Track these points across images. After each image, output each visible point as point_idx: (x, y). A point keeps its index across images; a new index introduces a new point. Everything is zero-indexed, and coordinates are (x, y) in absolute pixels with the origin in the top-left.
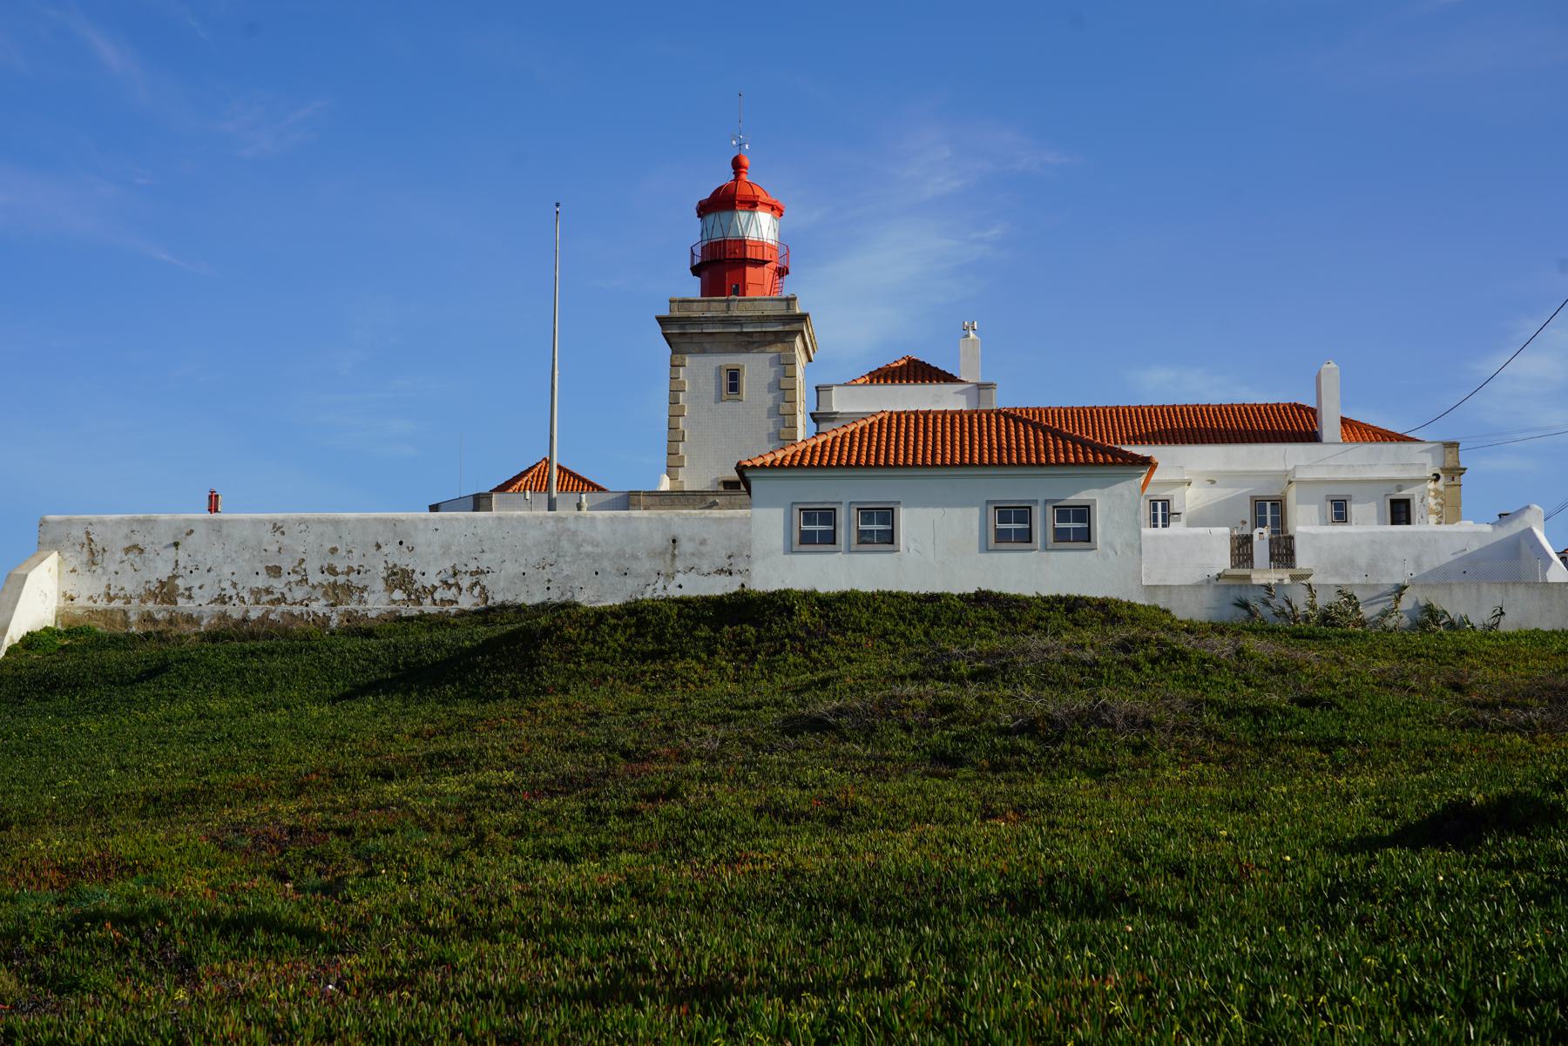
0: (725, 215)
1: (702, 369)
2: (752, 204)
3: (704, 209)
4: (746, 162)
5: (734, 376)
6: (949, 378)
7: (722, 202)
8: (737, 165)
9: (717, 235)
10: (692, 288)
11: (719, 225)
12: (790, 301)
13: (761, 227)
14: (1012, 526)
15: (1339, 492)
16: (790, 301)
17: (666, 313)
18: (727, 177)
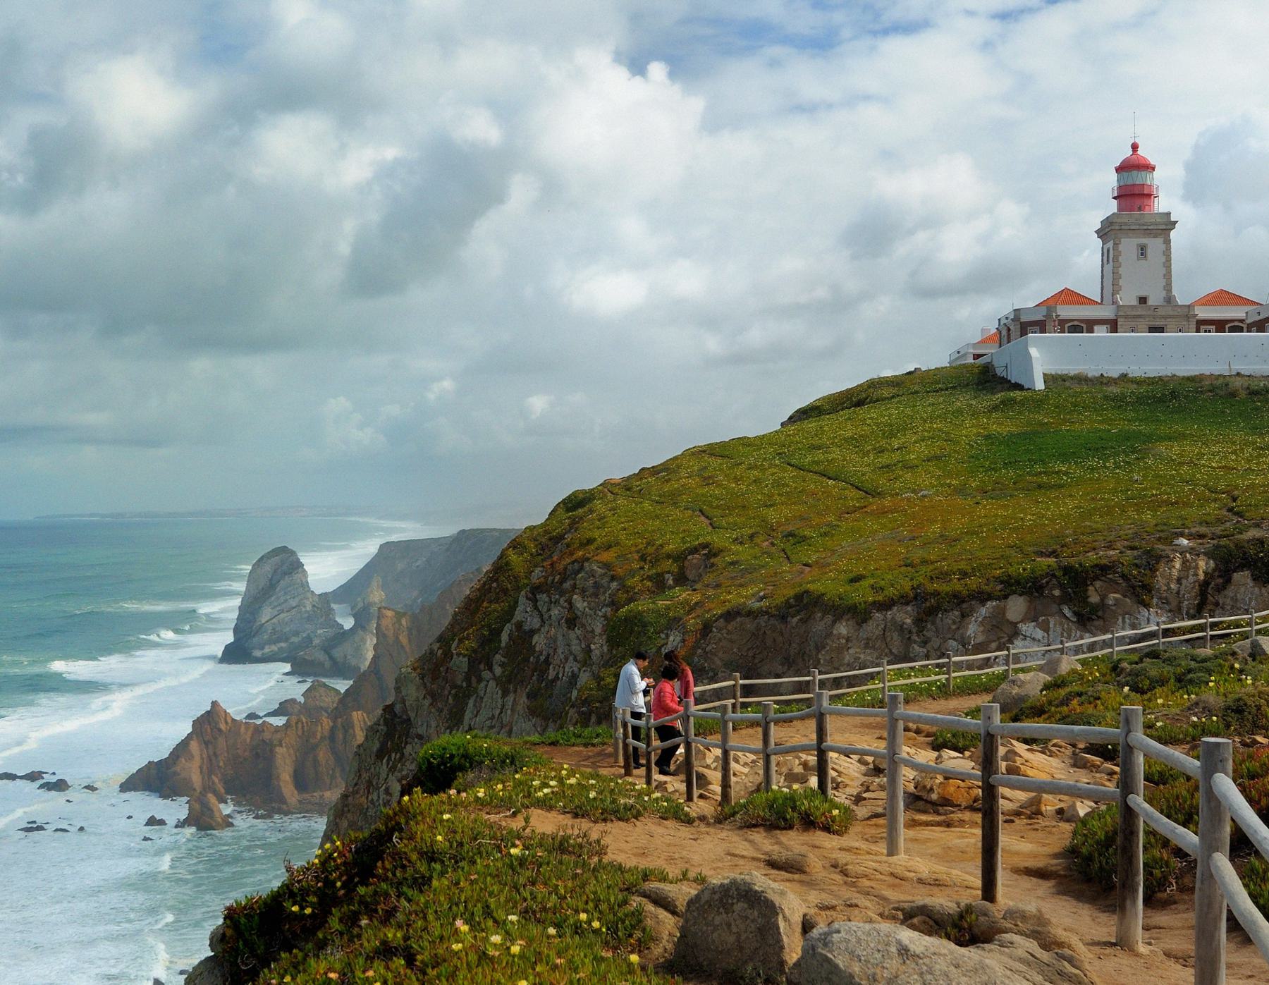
1: (1129, 246)
3: (1118, 170)
5: (1143, 251)
8: (1135, 147)
10: (1113, 207)
12: (1169, 214)
16: (1169, 214)
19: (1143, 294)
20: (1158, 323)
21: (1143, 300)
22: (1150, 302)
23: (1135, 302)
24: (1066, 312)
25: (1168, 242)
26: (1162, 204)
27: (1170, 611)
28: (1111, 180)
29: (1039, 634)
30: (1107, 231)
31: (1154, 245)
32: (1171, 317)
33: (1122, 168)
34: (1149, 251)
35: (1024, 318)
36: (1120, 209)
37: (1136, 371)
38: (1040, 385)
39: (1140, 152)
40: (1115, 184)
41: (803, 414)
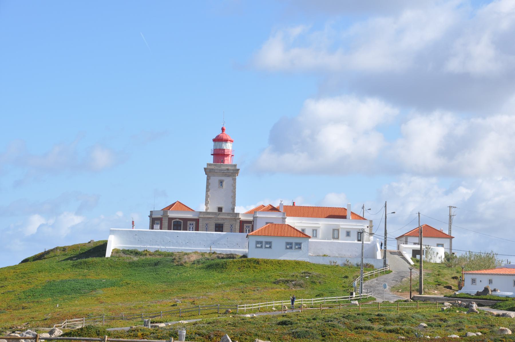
0: (220, 143)
1: (215, 180)
2: (226, 141)
3: (214, 140)
4: (225, 128)
5: (221, 182)
7: (218, 140)
8: (223, 129)
9: (218, 148)
10: (211, 160)
11: (219, 145)
13: (228, 147)
14: (290, 246)
15: (348, 230)
16: (235, 165)
17: (206, 167)
18: (219, 132)
19: (220, 206)
20: (220, 222)
21: (220, 209)
22: (223, 211)
23: (216, 211)
24: (172, 214)
25: (235, 180)
28: (211, 146)
31: (227, 181)
32: (226, 219)
35: (154, 216)
39: (225, 132)
40: (212, 148)
41: (25, 261)
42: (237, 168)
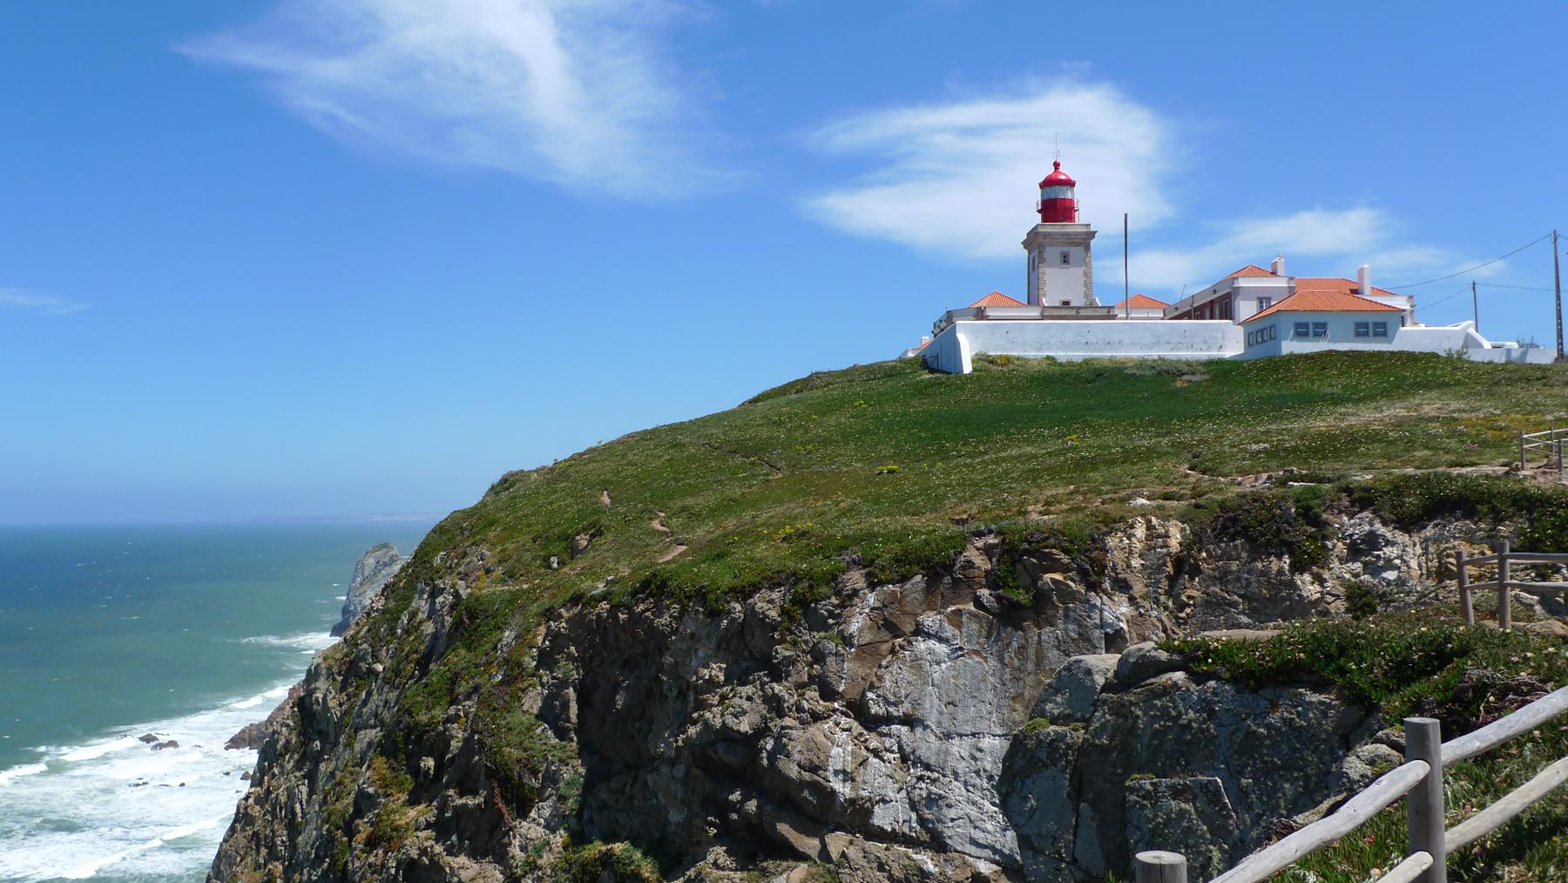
3: (1044, 185)
6: (1274, 273)
8: (1056, 165)
10: (1038, 218)
19: (1065, 299)
21: (1066, 303)
26: (1081, 217)
27: (1132, 600)
28: (1036, 196)
29: (949, 631)
30: (1033, 241)
31: (1075, 252)
33: (1048, 183)
34: (1071, 258)
36: (1044, 220)
37: (1062, 355)
38: (967, 368)
40: (1039, 198)
42: (1092, 229)
